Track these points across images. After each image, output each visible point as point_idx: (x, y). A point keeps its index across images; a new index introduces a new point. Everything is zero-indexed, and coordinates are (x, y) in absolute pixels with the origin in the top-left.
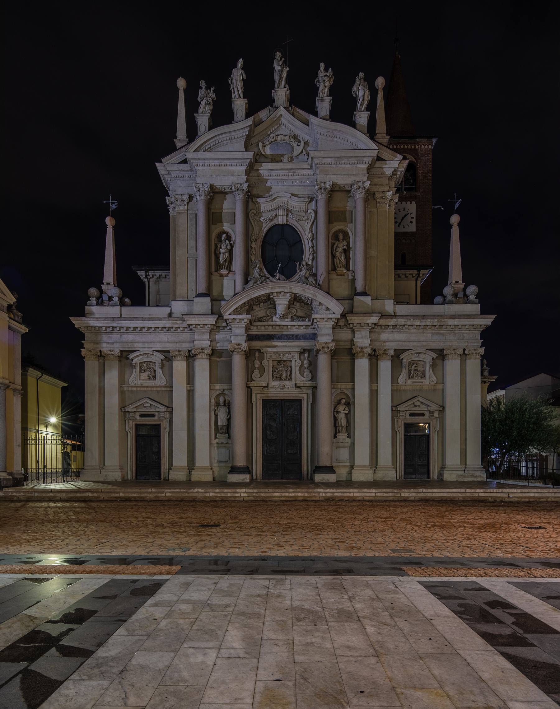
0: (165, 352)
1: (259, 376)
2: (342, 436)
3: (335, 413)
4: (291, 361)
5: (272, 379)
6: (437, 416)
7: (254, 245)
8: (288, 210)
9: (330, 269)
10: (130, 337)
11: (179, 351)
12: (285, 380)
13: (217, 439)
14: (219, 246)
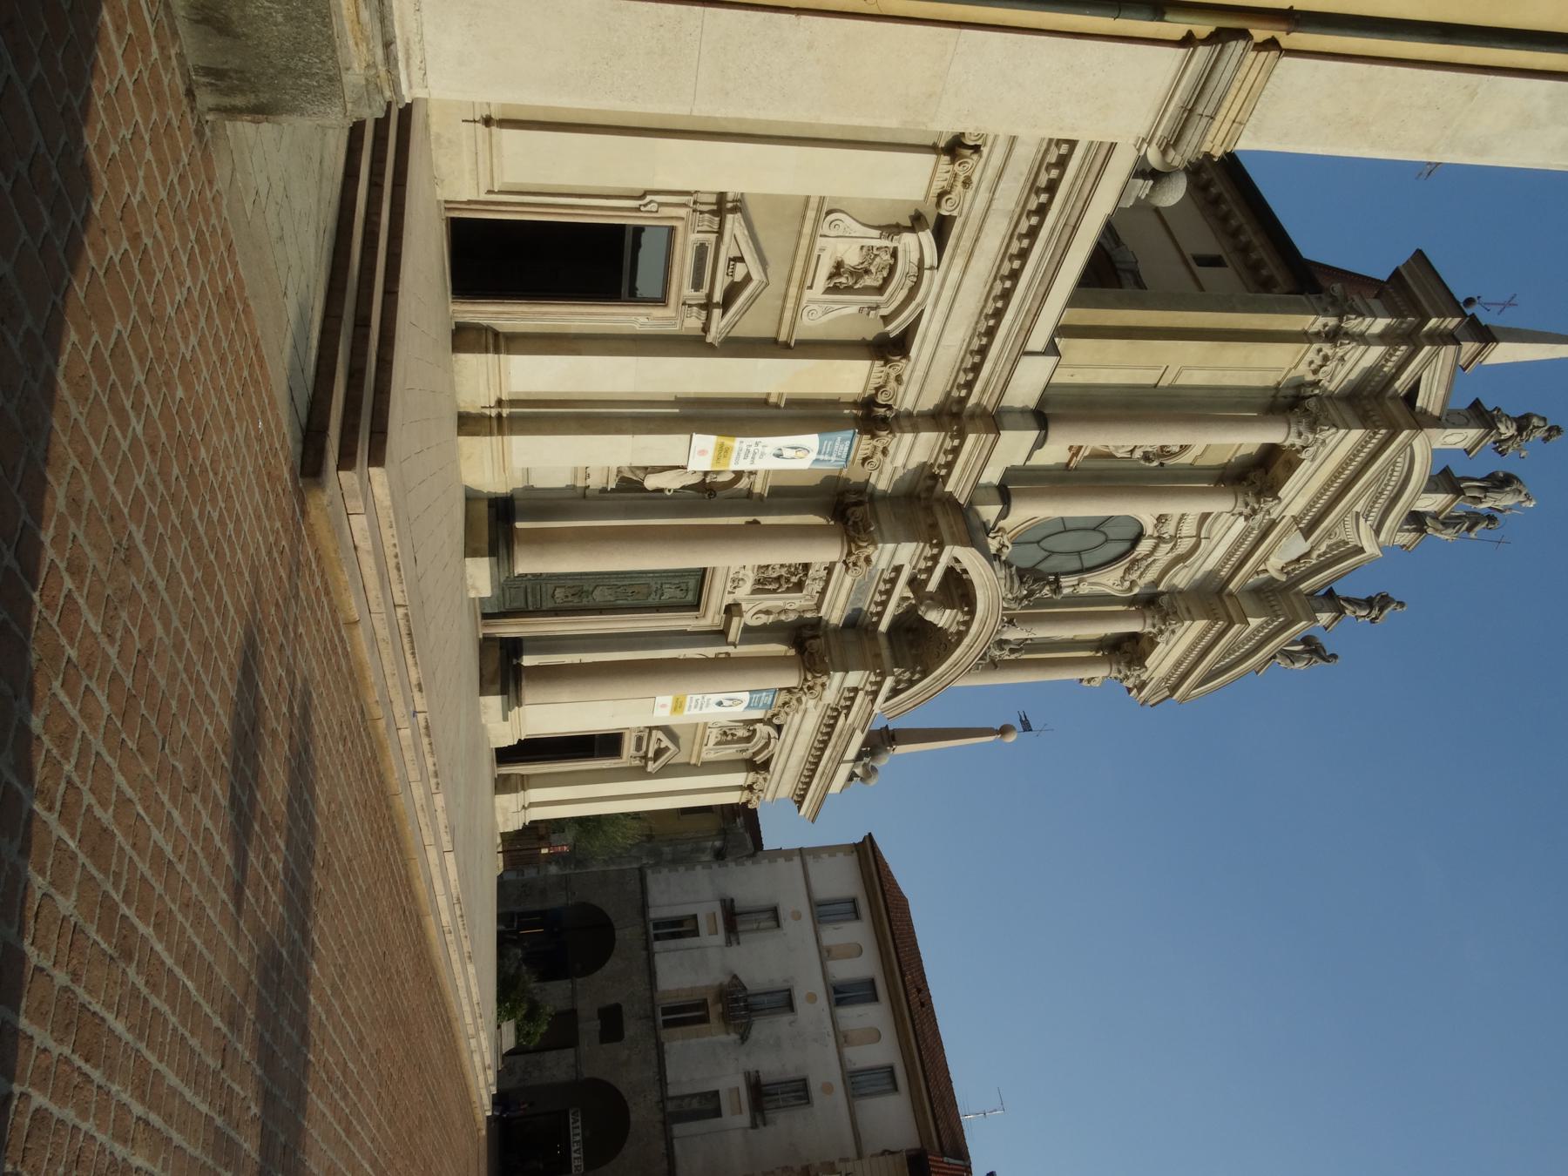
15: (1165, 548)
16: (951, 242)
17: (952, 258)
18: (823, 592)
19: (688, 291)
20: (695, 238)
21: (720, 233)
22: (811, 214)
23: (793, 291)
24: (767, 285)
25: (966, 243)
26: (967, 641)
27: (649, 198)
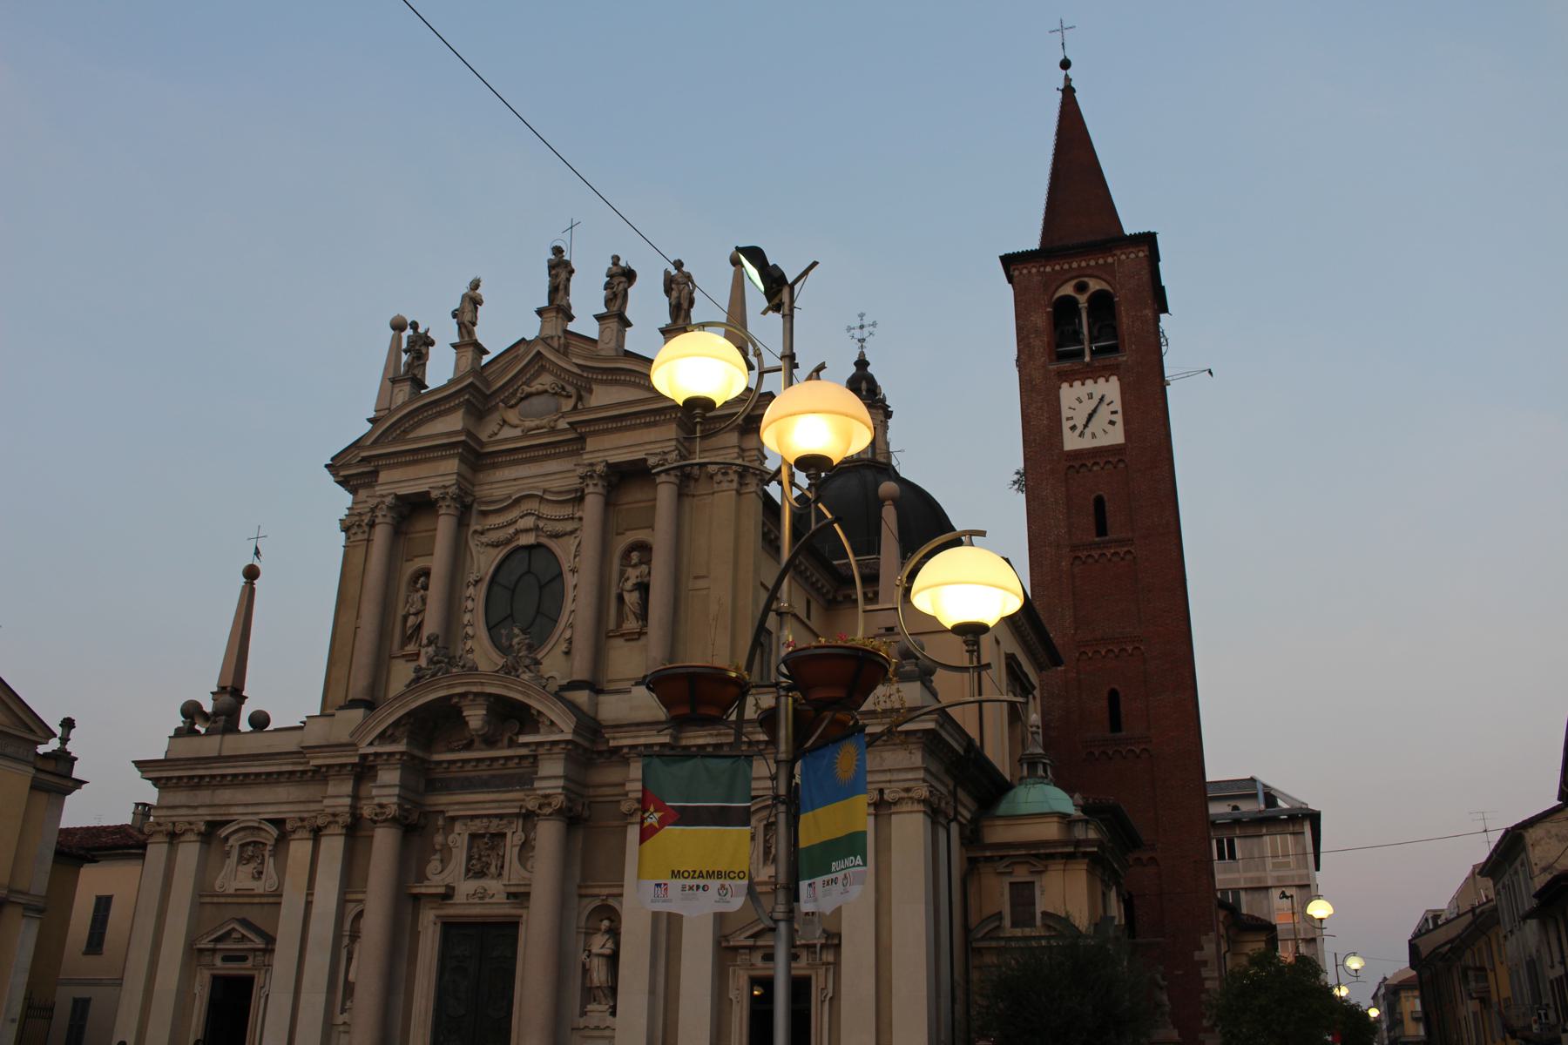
0: (278, 823)
1: (439, 869)
2: (598, 1009)
3: (587, 953)
4: (504, 835)
5: (466, 875)
6: (831, 958)
7: (471, 590)
8: (539, 517)
9: (612, 625)
10: (225, 795)
11: (302, 820)
12: (493, 878)
13: (345, 1014)
14: (410, 600)
15: (522, 524)
16: (224, 818)
17: (229, 814)
18: (500, 817)
19: (249, 963)
20: (218, 962)
21: (214, 951)
22: (215, 900)
23: (256, 900)
24: (234, 918)
25: (222, 811)
26: (475, 689)
27: (196, 991)
